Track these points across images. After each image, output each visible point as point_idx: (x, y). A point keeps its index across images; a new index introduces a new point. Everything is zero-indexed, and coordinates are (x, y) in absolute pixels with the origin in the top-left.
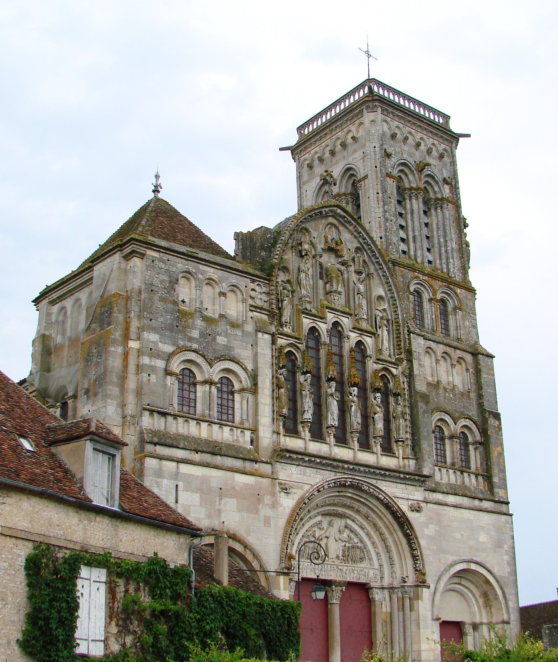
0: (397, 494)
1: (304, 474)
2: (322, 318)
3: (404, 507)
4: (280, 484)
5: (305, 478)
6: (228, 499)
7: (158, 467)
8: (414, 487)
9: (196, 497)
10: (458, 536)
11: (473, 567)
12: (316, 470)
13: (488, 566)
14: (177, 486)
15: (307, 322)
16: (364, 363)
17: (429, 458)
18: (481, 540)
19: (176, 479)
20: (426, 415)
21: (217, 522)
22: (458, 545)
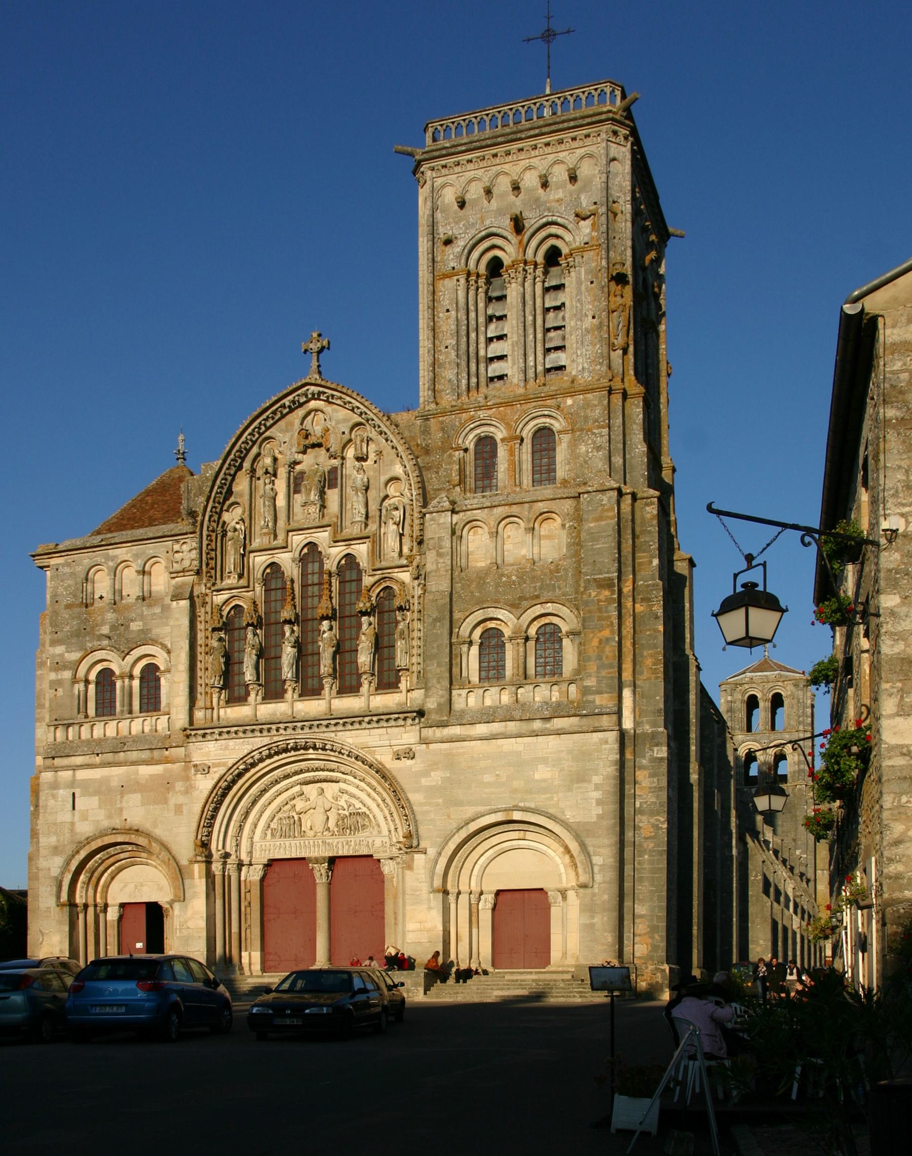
0: (370, 743)
1: (227, 748)
2: (286, 547)
3: (386, 759)
4: (195, 766)
5: (227, 752)
6: (131, 795)
7: (53, 779)
8: (402, 728)
9: (95, 801)
10: (488, 778)
11: (517, 816)
12: (242, 740)
13: (552, 811)
14: (74, 794)
15: (259, 561)
16: (360, 580)
17: (439, 682)
18: (537, 776)
19: (73, 788)
20: (438, 624)
21: (118, 821)
22: (487, 790)
